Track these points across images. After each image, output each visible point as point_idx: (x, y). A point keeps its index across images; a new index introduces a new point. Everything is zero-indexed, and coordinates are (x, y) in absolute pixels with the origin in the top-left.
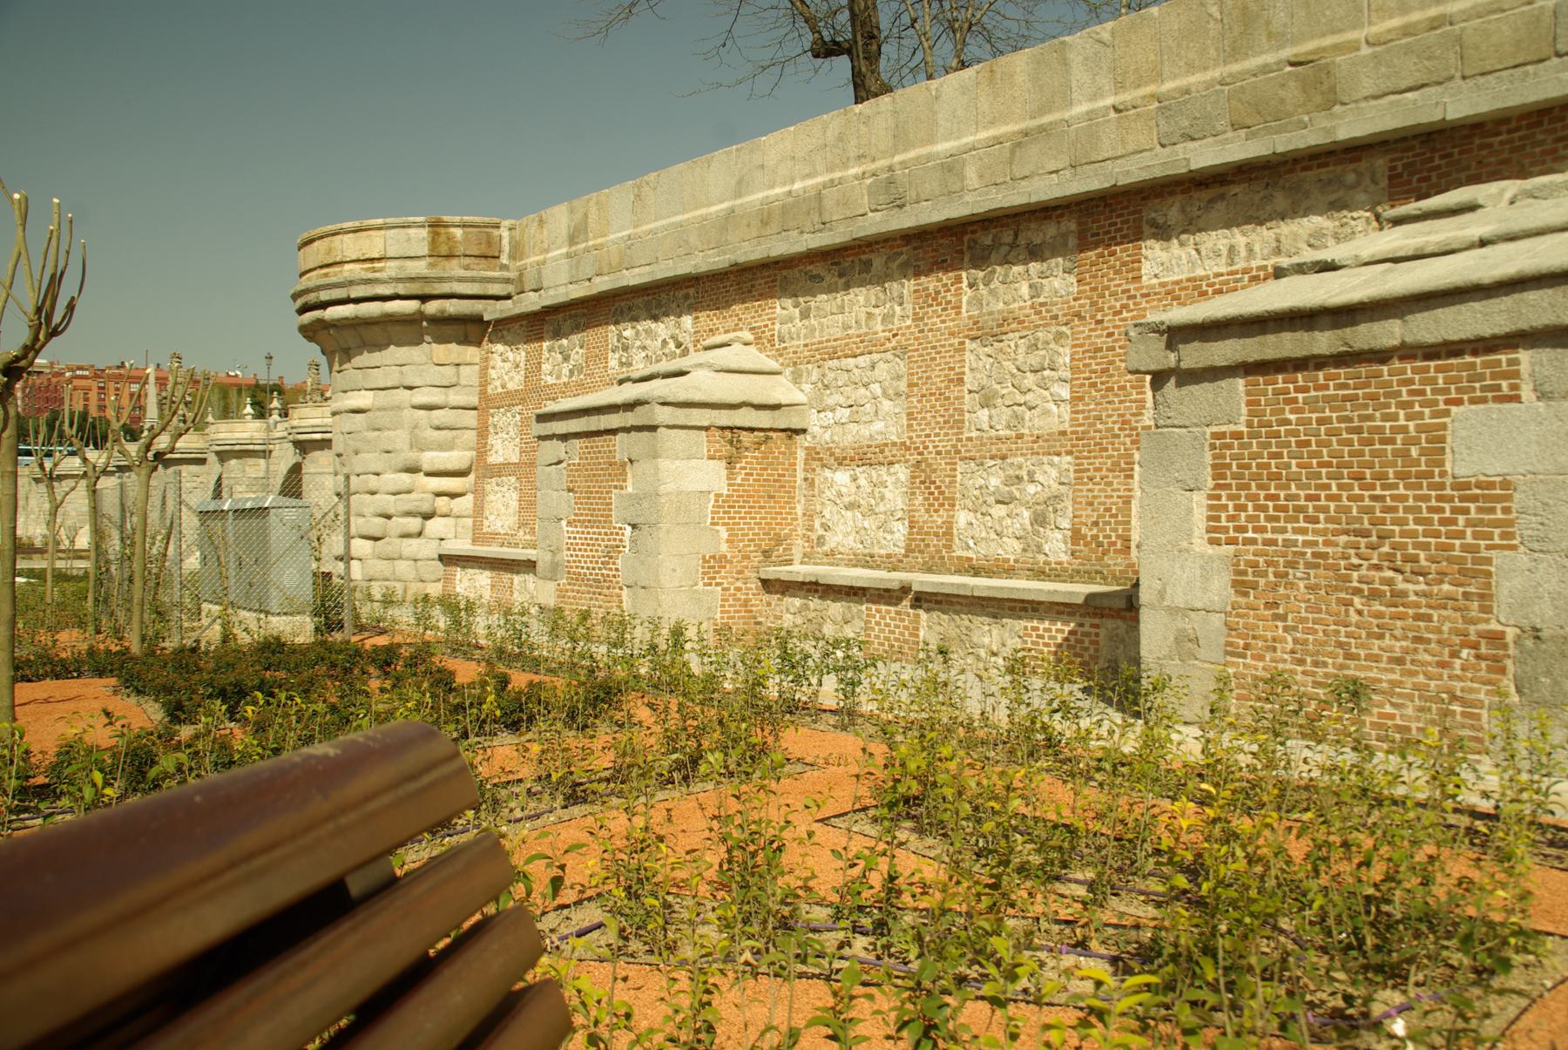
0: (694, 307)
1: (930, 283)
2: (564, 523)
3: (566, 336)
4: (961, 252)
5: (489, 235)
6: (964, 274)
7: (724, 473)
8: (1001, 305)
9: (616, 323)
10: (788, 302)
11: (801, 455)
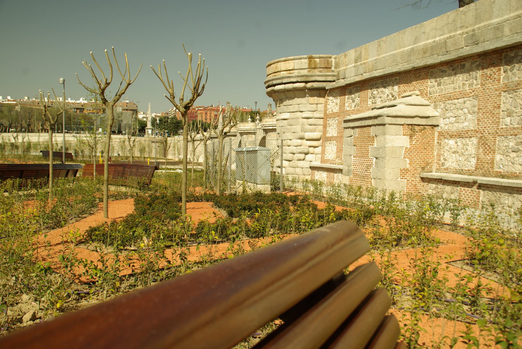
0: (398, 83)
1: (488, 71)
2: (352, 157)
3: (354, 94)
4: (501, 60)
5: (328, 61)
6: (502, 68)
7: (409, 140)
8: (517, 79)
9: (371, 89)
10: (433, 80)
11: (436, 134)
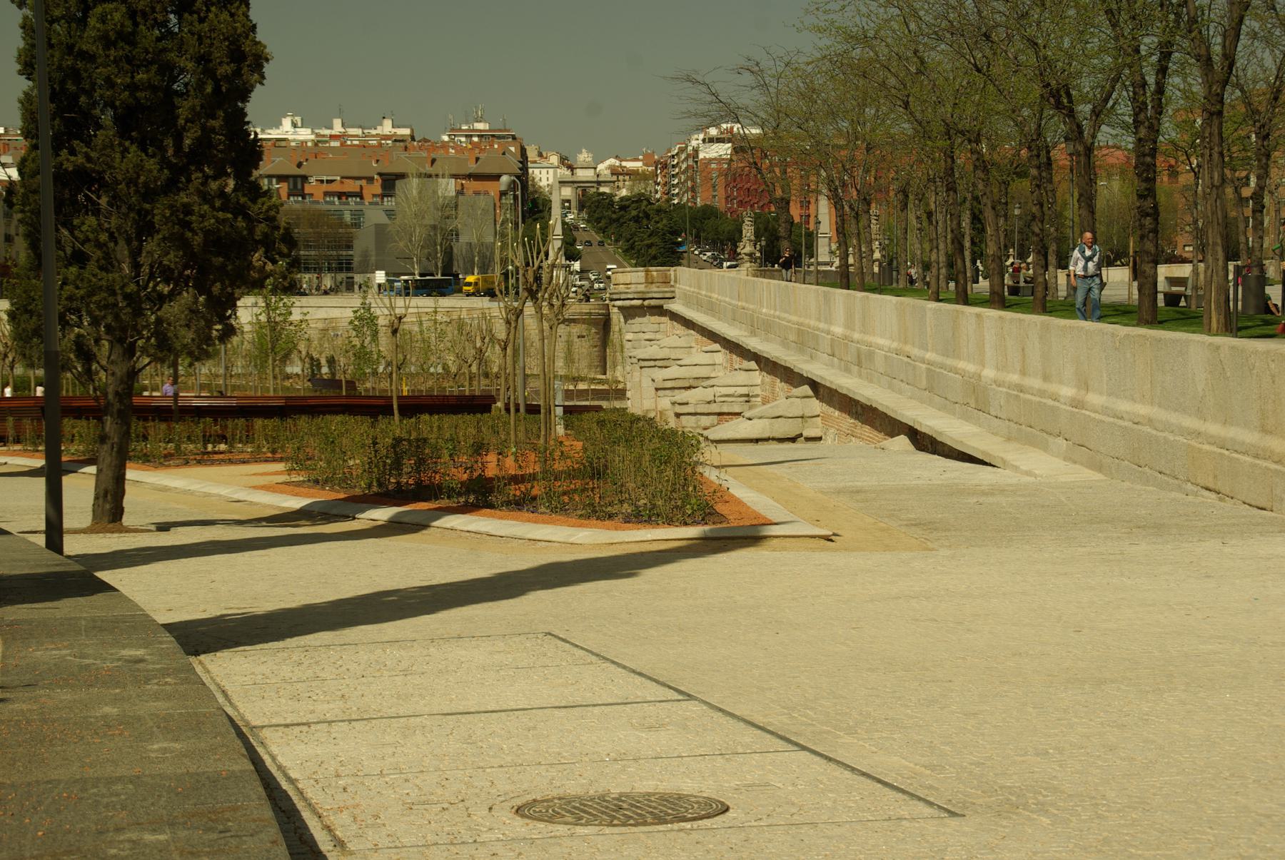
5: (666, 274)
